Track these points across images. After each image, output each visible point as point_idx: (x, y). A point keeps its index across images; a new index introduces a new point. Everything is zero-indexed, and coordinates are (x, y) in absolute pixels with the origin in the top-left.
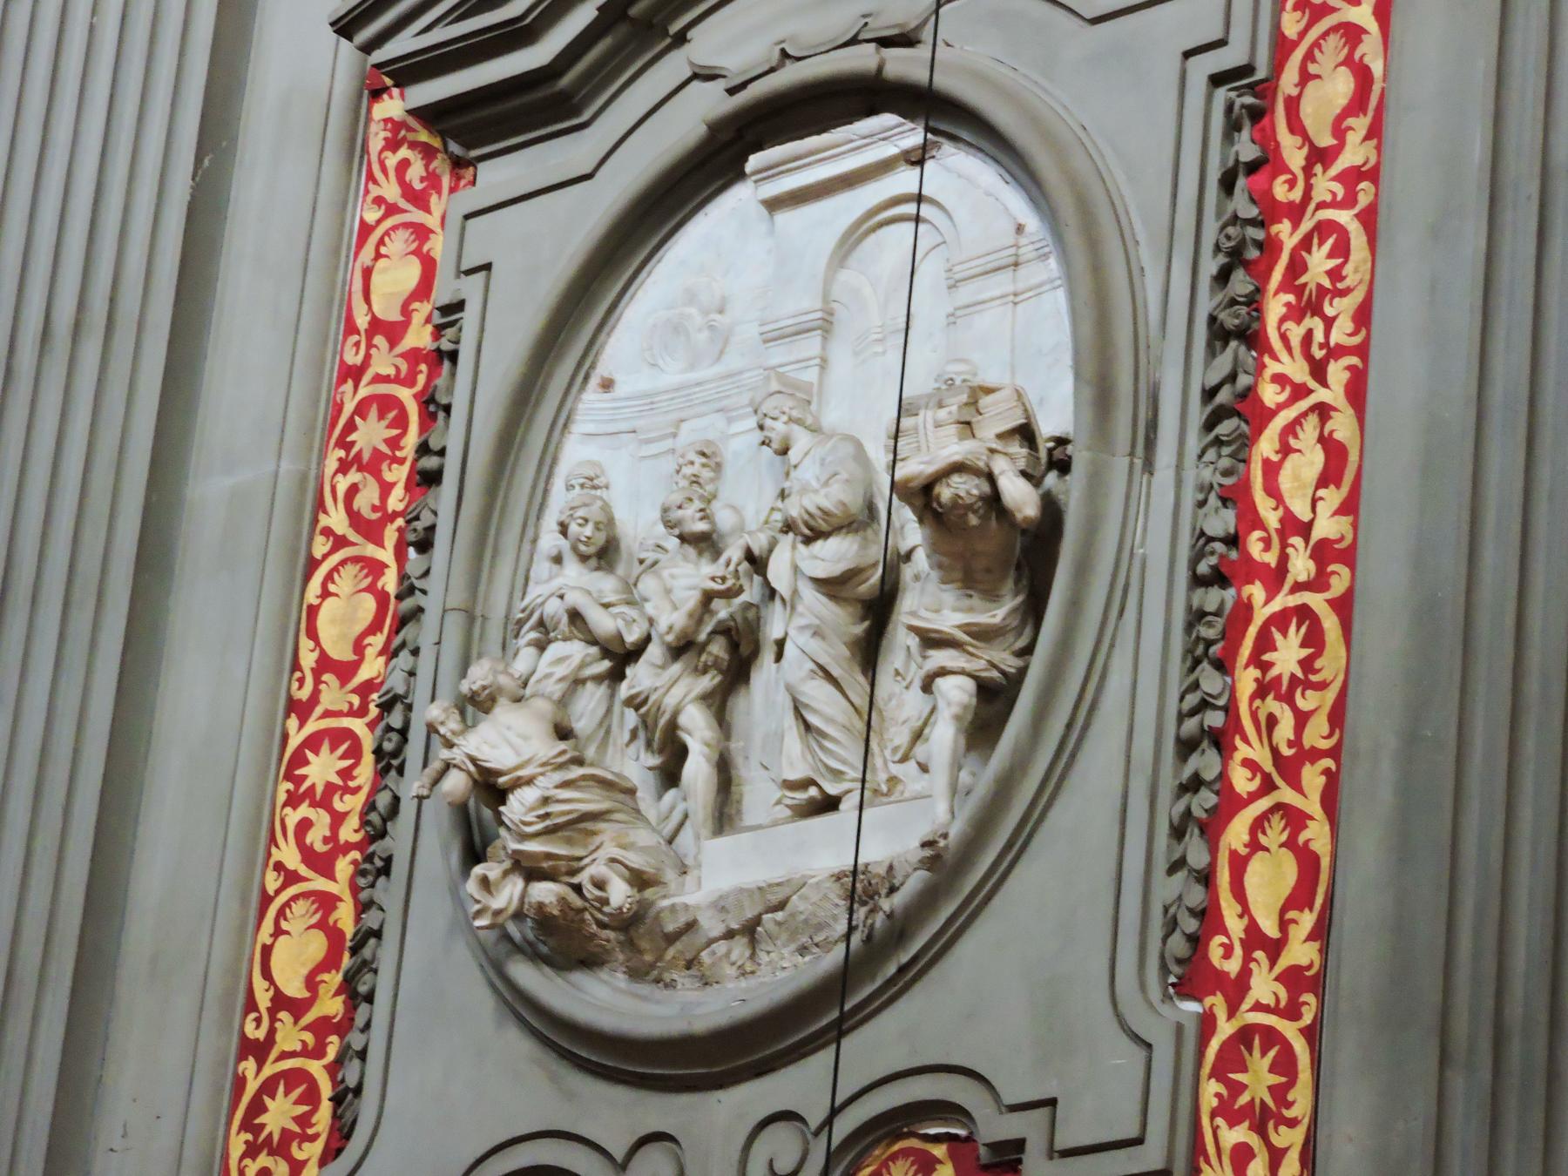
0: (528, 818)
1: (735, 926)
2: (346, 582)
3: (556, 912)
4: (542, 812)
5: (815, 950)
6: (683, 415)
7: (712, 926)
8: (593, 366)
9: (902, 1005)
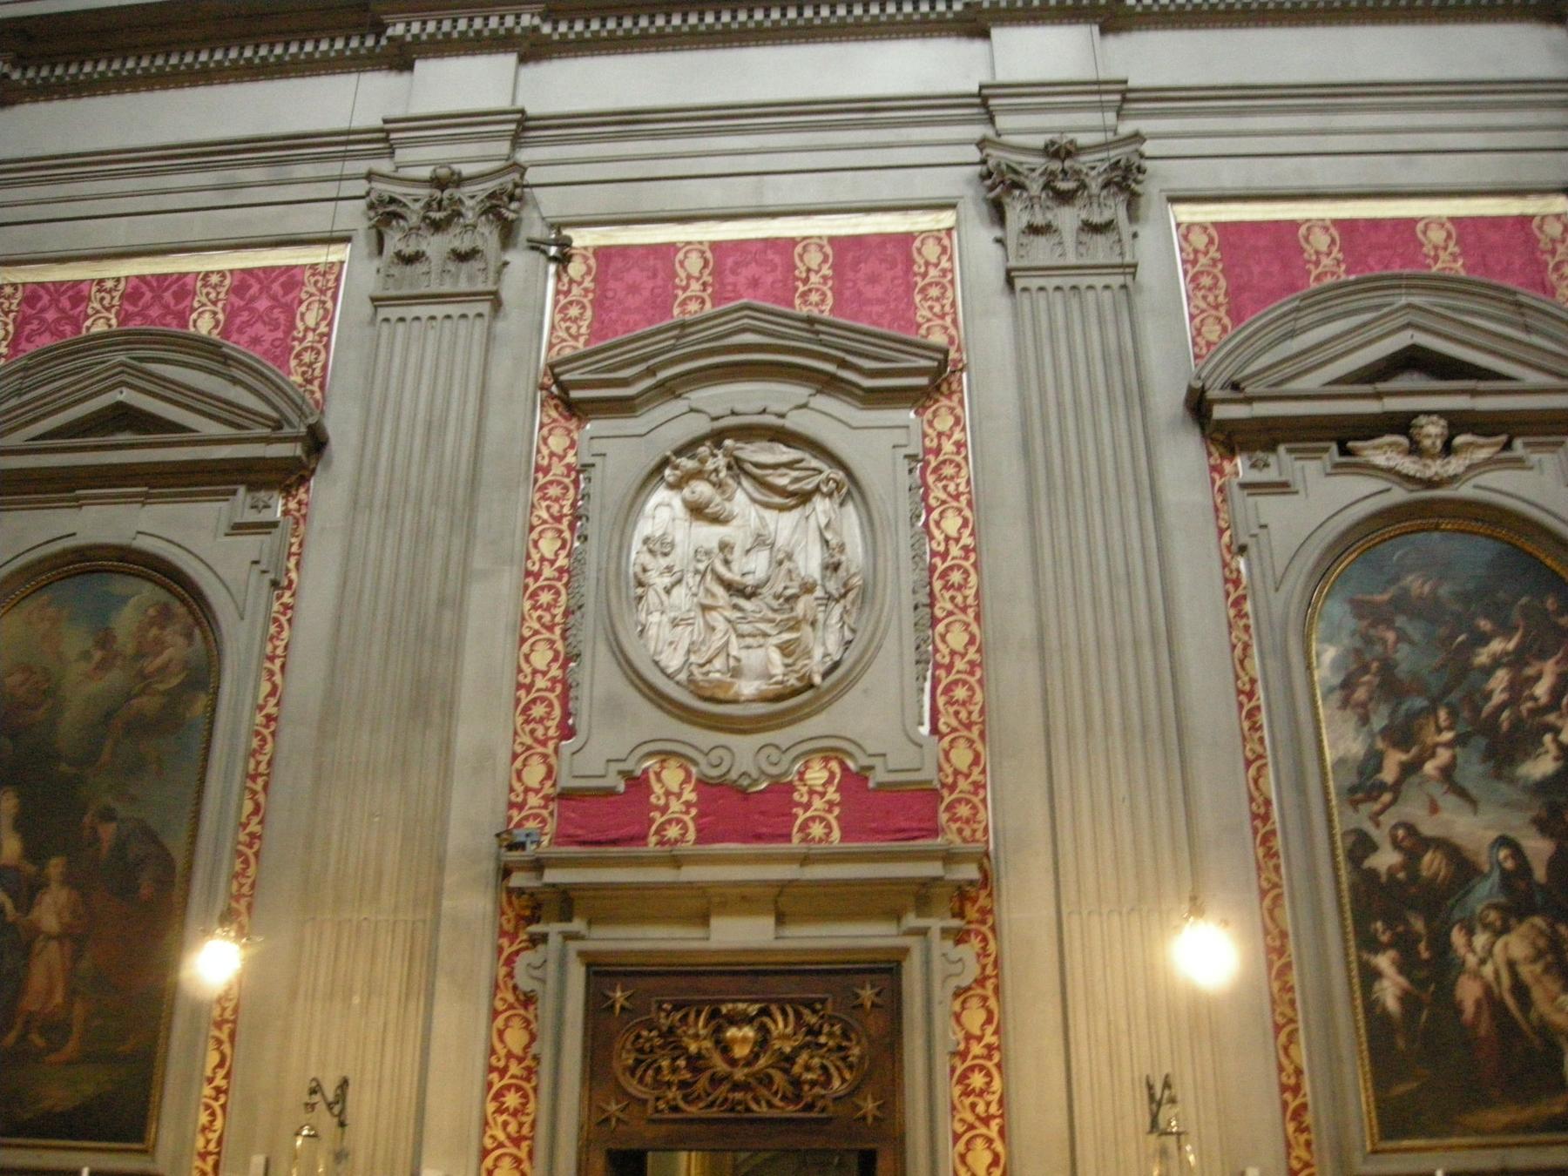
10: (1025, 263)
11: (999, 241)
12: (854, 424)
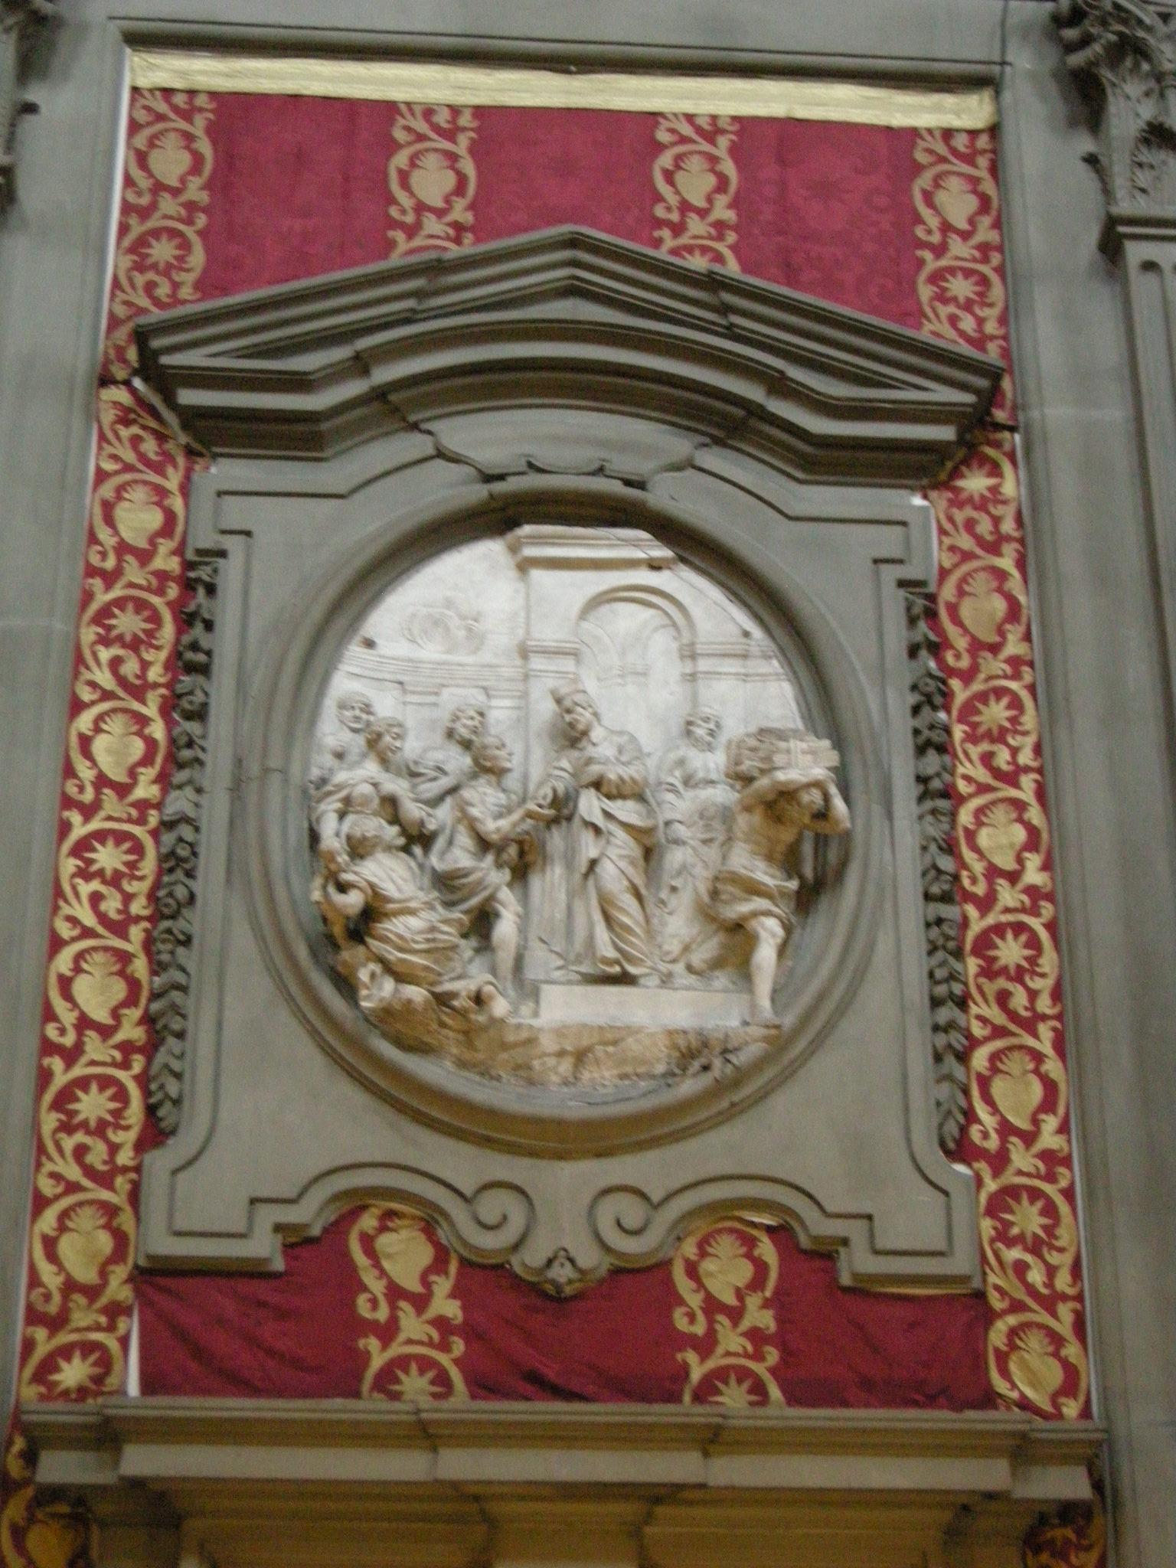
0: (418, 938)
1: (569, 1048)
2: (116, 725)
3: (420, 1009)
4: (430, 936)
5: (635, 1078)
6: (445, 682)
7: (548, 1044)
10: (1142, 207)
11: (1091, 160)
12: (790, 513)
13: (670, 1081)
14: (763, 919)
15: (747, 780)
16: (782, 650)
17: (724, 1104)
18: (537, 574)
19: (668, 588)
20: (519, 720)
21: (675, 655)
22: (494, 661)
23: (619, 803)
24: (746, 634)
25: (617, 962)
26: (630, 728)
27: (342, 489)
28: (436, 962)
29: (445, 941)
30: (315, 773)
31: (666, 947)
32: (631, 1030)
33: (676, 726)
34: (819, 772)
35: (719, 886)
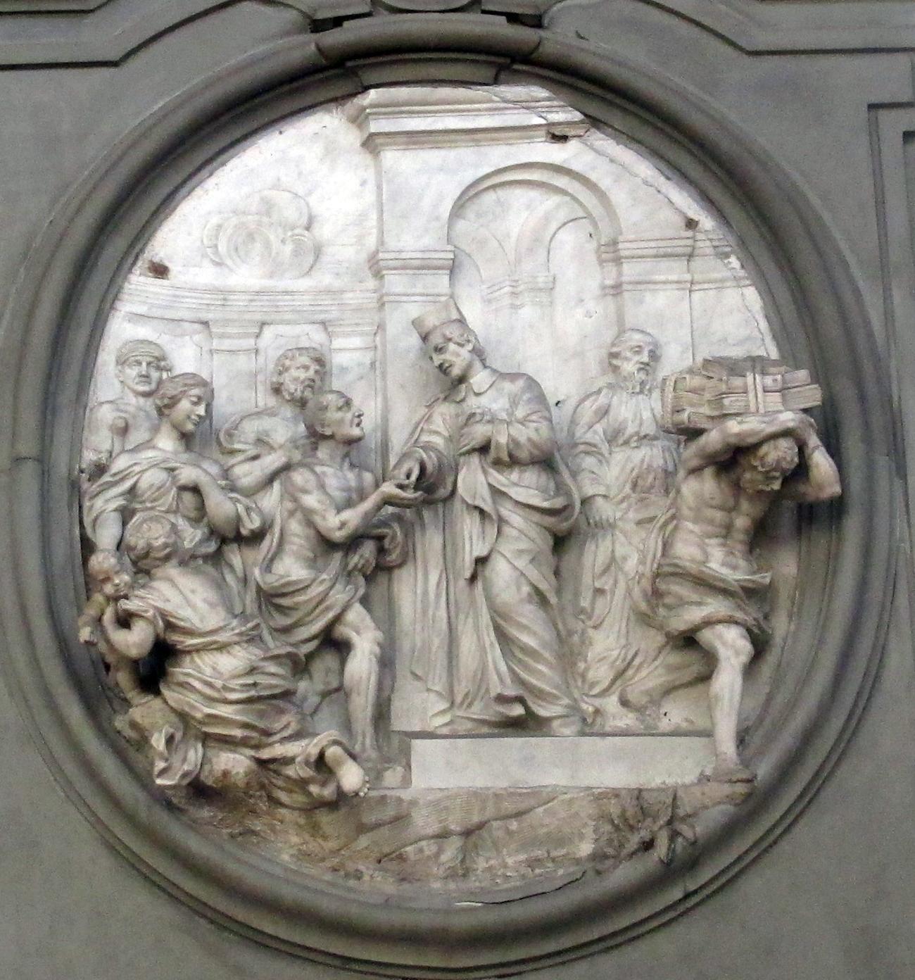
4: (250, 680)
5: (550, 865)
7: (424, 822)
8: (142, 251)
9: (679, 929)
13: (599, 867)
14: (720, 628)
15: (693, 433)
16: (743, 243)
17: (676, 893)
18: (391, 157)
19: (576, 166)
20: (373, 364)
21: (592, 258)
22: (338, 284)
23: (515, 476)
24: (691, 224)
25: (520, 700)
26: (529, 369)
27: (113, 55)
28: (262, 715)
29: (271, 687)
30: (89, 457)
31: (591, 675)
32: (541, 796)
33: (594, 358)
34: (788, 418)
35: (662, 586)
